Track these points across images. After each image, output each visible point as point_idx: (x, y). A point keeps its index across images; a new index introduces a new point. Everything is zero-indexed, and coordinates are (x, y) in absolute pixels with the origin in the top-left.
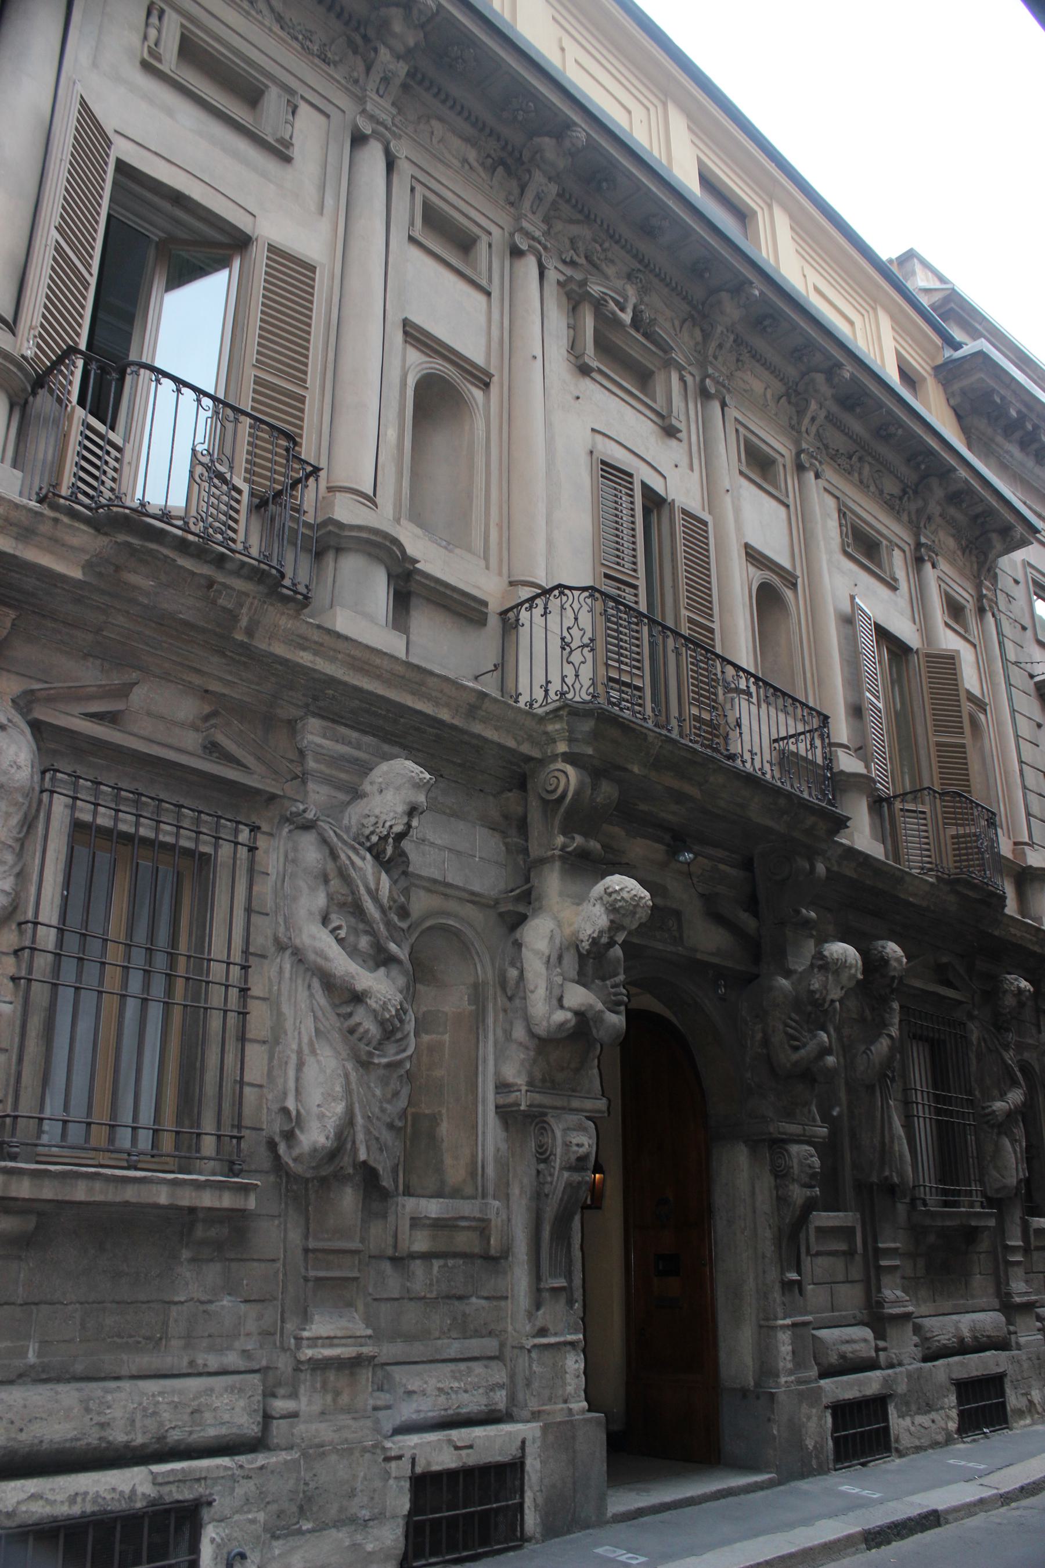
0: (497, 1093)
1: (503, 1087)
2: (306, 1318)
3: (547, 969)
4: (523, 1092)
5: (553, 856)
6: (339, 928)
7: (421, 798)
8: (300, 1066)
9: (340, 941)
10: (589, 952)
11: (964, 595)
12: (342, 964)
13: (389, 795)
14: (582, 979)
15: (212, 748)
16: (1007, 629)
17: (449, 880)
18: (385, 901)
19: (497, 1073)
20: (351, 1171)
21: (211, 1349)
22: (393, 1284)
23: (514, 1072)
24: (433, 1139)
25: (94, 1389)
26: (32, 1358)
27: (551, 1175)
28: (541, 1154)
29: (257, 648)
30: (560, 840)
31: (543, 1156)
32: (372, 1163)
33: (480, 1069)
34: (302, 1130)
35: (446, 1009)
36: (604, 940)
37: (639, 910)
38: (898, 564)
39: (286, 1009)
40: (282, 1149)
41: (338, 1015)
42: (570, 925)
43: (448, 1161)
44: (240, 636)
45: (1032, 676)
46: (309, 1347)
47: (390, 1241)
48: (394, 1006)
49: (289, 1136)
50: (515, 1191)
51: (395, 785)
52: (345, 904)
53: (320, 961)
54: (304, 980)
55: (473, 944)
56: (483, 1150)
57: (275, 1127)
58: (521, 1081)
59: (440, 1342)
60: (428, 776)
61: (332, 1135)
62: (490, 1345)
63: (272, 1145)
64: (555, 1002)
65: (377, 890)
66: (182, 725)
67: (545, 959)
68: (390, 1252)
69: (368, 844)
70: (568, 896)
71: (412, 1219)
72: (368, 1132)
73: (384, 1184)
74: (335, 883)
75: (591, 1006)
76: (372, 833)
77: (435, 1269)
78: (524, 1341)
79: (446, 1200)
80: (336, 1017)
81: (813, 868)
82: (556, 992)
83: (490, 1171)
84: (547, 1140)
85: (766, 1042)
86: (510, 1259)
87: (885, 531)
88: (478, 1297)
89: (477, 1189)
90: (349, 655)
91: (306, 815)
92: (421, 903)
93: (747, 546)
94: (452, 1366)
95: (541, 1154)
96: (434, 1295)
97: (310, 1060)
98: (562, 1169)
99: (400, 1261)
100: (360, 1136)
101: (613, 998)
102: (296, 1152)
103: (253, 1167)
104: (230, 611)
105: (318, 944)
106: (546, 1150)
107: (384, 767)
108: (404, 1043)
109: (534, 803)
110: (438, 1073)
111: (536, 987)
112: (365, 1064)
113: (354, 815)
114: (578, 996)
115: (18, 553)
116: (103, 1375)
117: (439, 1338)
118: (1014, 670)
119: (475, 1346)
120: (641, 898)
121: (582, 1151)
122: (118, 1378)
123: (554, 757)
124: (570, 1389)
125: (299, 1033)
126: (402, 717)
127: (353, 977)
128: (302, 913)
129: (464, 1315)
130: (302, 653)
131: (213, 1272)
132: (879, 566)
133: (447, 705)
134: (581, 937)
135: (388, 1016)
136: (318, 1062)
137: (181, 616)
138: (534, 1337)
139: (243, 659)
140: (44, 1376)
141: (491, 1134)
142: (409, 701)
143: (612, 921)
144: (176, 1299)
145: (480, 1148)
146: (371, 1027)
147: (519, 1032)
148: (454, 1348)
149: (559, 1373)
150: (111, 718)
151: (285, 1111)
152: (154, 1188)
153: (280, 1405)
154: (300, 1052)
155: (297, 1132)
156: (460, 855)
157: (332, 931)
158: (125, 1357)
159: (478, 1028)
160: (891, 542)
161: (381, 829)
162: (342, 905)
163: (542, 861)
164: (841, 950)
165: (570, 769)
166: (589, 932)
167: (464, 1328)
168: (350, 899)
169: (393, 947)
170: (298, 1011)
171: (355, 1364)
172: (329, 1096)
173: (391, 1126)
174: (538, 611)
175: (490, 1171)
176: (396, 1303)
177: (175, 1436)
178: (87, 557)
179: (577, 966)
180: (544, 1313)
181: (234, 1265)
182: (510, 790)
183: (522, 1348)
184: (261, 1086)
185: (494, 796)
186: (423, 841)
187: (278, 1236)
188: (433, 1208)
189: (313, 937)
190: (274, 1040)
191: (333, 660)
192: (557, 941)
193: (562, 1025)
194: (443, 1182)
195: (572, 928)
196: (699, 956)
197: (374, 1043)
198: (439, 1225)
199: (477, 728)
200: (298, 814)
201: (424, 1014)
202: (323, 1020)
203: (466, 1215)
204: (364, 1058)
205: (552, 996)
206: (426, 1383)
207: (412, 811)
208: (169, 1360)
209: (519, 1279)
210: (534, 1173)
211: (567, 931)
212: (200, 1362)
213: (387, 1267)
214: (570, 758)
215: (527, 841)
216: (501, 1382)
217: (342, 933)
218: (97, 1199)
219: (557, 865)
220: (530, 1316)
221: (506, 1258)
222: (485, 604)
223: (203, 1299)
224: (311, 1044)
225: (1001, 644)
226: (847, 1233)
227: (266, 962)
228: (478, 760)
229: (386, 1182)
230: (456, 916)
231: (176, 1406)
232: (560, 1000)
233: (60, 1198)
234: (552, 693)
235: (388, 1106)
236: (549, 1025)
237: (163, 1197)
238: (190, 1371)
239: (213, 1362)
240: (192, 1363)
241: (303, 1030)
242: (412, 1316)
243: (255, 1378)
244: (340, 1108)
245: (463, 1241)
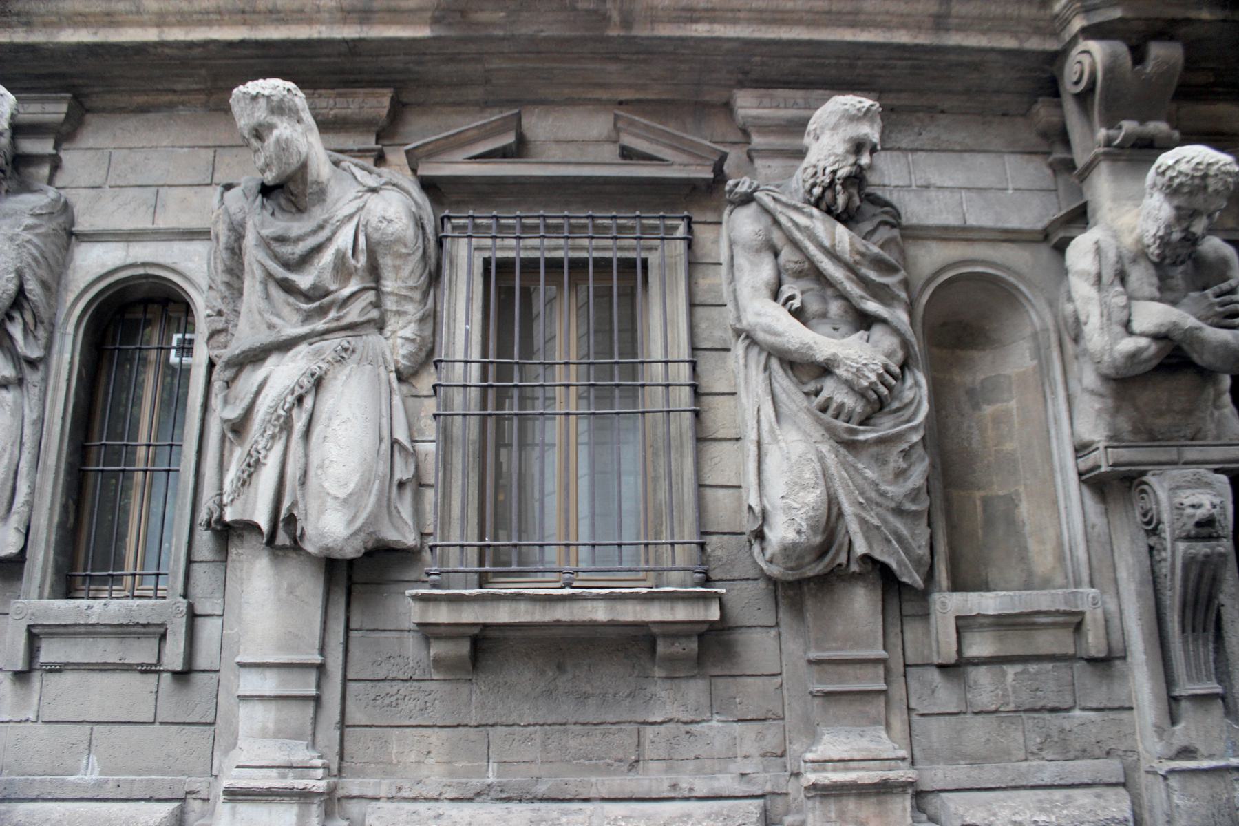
0: (1077, 458)
1: (1081, 449)
2: (813, 736)
3: (1099, 290)
4: (1102, 449)
5: (1096, 156)
6: (792, 298)
7: (872, 132)
9: (798, 314)
10: (1162, 257)
12: (794, 334)
13: (825, 139)
14: (1166, 293)
15: (628, 154)
17: (972, 221)
18: (847, 256)
19: (1072, 434)
20: (854, 568)
21: (699, 771)
22: (945, 695)
23: (1092, 427)
24: (1012, 522)
26: (491, 778)
27: (1165, 549)
28: (1148, 523)
29: (635, 37)
30: (1102, 133)
31: (1152, 528)
32: (878, 555)
33: (1053, 432)
34: (771, 529)
35: (1008, 371)
36: (1176, 236)
37: (1211, 181)
41: (807, 394)
42: (1132, 231)
43: (1033, 545)
44: (613, 32)
46: (815, 771)
48: (873, 371)
49: (760, 535)
50: (1123, 574)
52: (801, 272)
53: (770, 339)
54: (758, 363)
55: (1017, 289)
56: (1069, 529)
59: (1024, 764)
60: (867, 102)
61: (805, 528)
62: (1111, 769)
64: (1118, 329)
65: (833, 246)
66: (597, 142)
67: (1092, 280)
68: (936, 661)
69: (812, 200)
70: (1129, 198)
71: (957, 618)
72: (863, 522)
73: (905, 579)
75: (1175, 324)
76: (814, 185)
77: (1010, 678)
78: (1156, 764)
79: (1035, 592)
80: (802, 396)
82: (1124, 316)
84: (1149, 503)
86: (1129, 659)
88: (1083, 709)
89: (1067, 577)
90: (750, 10)
91: (738, 189)
92: (930, 258)
94: (1042, 794)
95: (1148, 523)
96: (1011, 707)
98: (1175, 540)
99: (956, 669)
100: (854, 527)
101: (1221, 309)
103: (736, 575)
104: (595, 12)
105: (764, 321)
106: (1152, 518)
107: (818, 112)
108: (907, 413)
109: (1070, 107)
110: (1008, 446)
111: (1088, 317)
112: (851, 446)
114: (1153, 315)
115: (363, 35)
116: (568, 797)
117: (1026, 760)
119: (1083, 769)
120: (1209, 164)
121: (1200, 514)
122: (587, 800)
125: (759, 422)
126: (859, 58)
127: (810, 348)
129: (1062, 731)
130: (694, 26)
131: (695, 690)
133: (904, 26)
134: (1148, 240)
135: (865, 384)
136: (780, 448)
137: (543, 34)
138: (1171, 759)
139: (642, 57)
140: (504, 796)
141: (1075, 509)
142: (848, 35)
143: (1178, 208)
144: (651, 720)
145: (1065, 527)
148: (1049, 771)
152: (589, 605)
154: (759, 444)
155: (766, 530)
156: (961, 190)
157: (784, 304)
158: (593, 779)
159: (1043, 384)
161: (822, 178)
162: (799, 275)
163: (1090, 167)
166: (1153, 232)
167: (1065, 748)
168: (807, 265)
169: (872, 306)
171: (884, 789)
172: (797, 485)
173: (899, 511)
176: (953, 718)
178: (429, 14)
179: (1155, 280)
180: (1186, 728)
181: (720, 682)
182: (1036, 102)
183: (1155, 773)
184: (739, 487)
185: (1024, 115)
186: (927, 187)
187: (770, 646)
189: (758, 314)
191: (735, 22)
192: (1111, 255)
193: (1133, 356)
194: (1030, 574)
195: (1135, 235)
197: (856, 418)
199: (954, 39)
200: (731, 191)
201: (982, 382)
202: (788, 403)
203: (1044, 608)
204: (846, 437)
206: (994, 815)
207: (858, 146)
208: (646, 783)
209: (1141, 682)
210: (1145, 550)
212: (684, 785)
213: (935, 676)
214: (1091, 32)
216: (1119, 816)
218: (522, 620)
221: (1124, 658)
223: (685, 719)
224: (772, 431)
227: (728, 354)
229: (913, 578)
232: (1127, 326)
233: (481, 621)
235: (888, 488)
236: (1114, 360)
238: (672, 795)
240: (674, 786)
241: (763, 418)
242: (978, 732)
243: (754, 806)
244: (814, 497)
245: (1046, 642)
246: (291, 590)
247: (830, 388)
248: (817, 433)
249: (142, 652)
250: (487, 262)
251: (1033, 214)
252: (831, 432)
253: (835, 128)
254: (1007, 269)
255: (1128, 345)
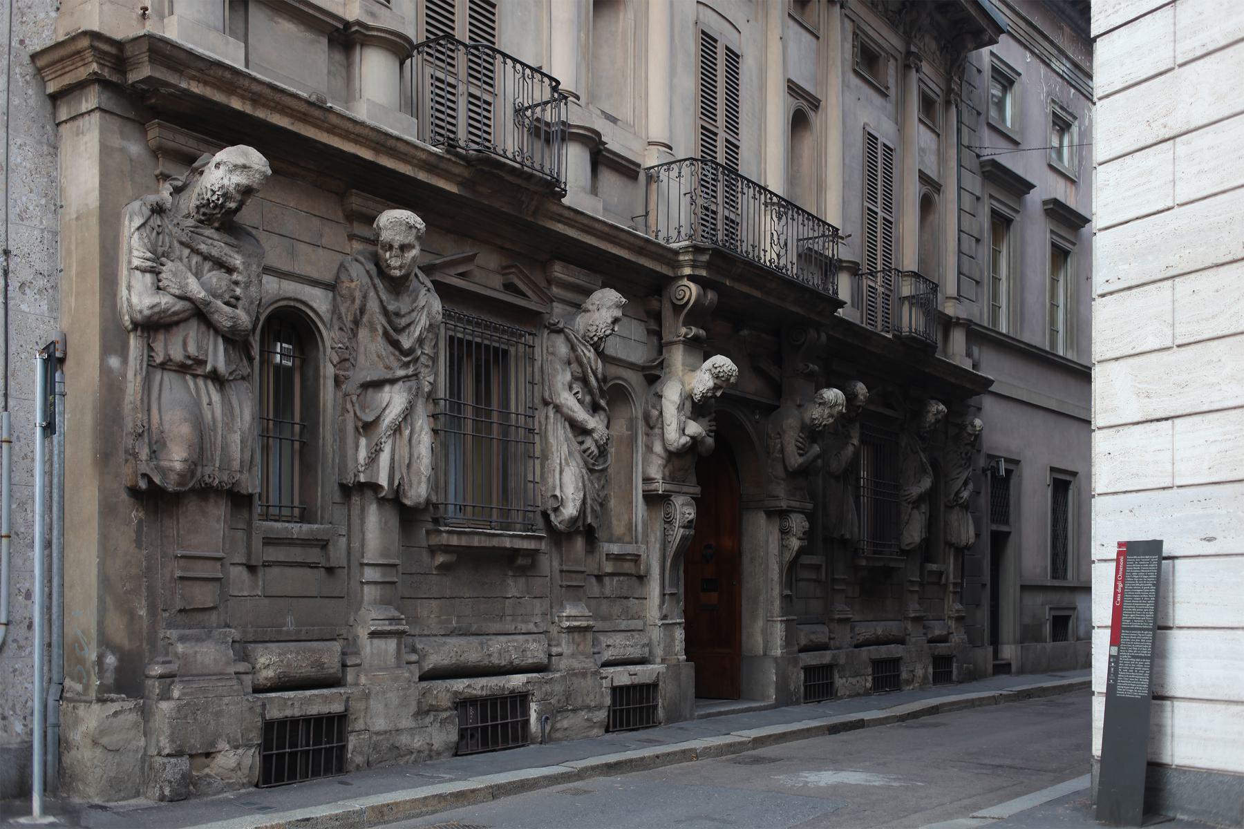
1: (647, 480)
2: (562, 607)
8: (561, 472)
11: (935, 88)
12: (581, 414)
16: (965, 118)
18: (600, 376)
22: (594, 588)
23: (655, 471)
25: (484, 638)
30: (684, 330)
31: (668, 521)
38: (891, 73)
39: (551, 440)
40: (553, 517)
45: (978, 156)
47: (596, 566)
49: (556, 510)
51: (605, 306)
57: (552, 504)
58: (658, 476)
63: (545, 515)
74: (575, 366)
81: (819, 337)
83: (640, 528)
85: (782, 451)
87: (885, 45)
93: (789, 81)
97: (566, 469)
100: (589, 510)
102: (560, 518)
112: (591, 471)
113: (581, 322)
114: (694, 428)
118: (965, 151)
121: (691, 517)
123: (683, 277)
124: (677, 648)
128: (560, 385)
132: (875, 76)
133: (628, 249)
146: (593, 448)
147: (658, 448)
149: (673, 640)
150: (462, 275)
151: (555, 496)
153: (555, 650)
160: (887, 53)
164: (833, 394)
165: (692, 285)
170: (559, 441)
172: (577, 488)
174: (674, 174)
175: (640, 528)
177: (516, 662)
188: (615, 549)
190: (545, 457)
193: (684, 445)
196: (748, 396)
198: (619, 558)
205: (678, 429)
207: (616, 321)
209: (654, 589)
211: (688, 388)
213: (593, 580)
215: (660, 326)
217: (580, 396)
219: (681, 347)
220: (661, 607)
222: (639, 166)
225: (959, 130)
226: (817, 568)
228: (641, 277)
230: (625, 380)
231: (515, 648)
234: (683, 234)
237: (507, 543)
239: (524, 628)
245: (628, 567)
246: (386, 523)
247: (589, 443)
248: (582, 464)
249: (314, 555)
250: (452, 338)
251: (638, 354)
252: (586, 463)
253: (609, 308)
254: (630, 384)
255: (684, 440)
